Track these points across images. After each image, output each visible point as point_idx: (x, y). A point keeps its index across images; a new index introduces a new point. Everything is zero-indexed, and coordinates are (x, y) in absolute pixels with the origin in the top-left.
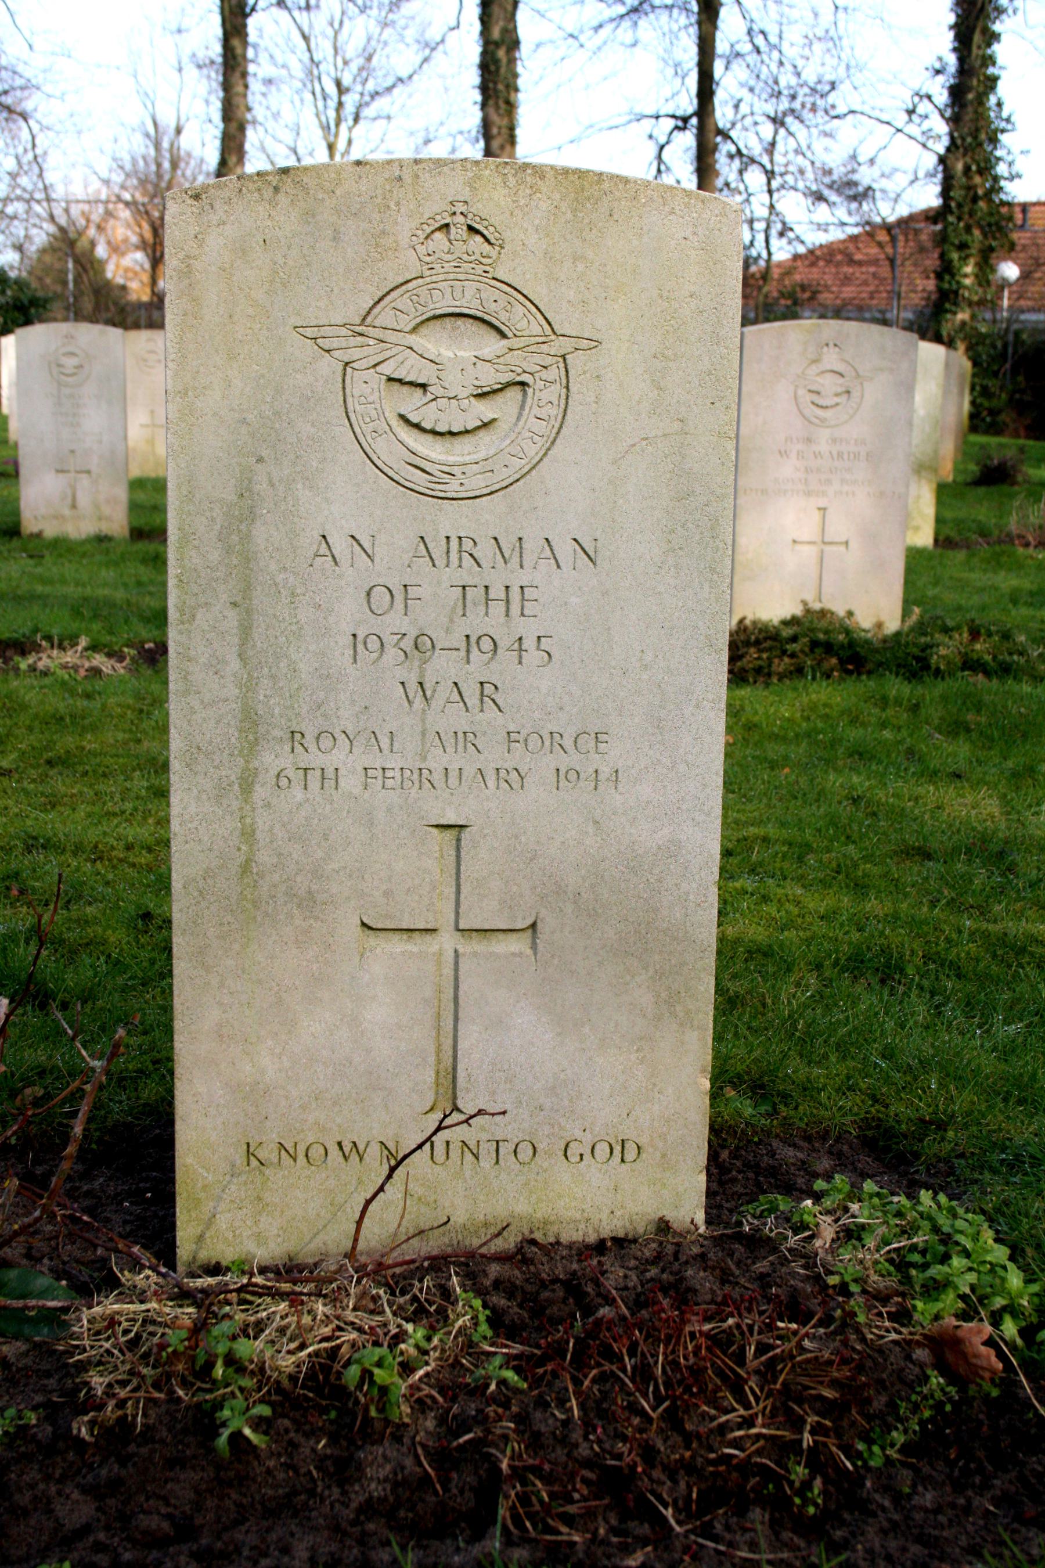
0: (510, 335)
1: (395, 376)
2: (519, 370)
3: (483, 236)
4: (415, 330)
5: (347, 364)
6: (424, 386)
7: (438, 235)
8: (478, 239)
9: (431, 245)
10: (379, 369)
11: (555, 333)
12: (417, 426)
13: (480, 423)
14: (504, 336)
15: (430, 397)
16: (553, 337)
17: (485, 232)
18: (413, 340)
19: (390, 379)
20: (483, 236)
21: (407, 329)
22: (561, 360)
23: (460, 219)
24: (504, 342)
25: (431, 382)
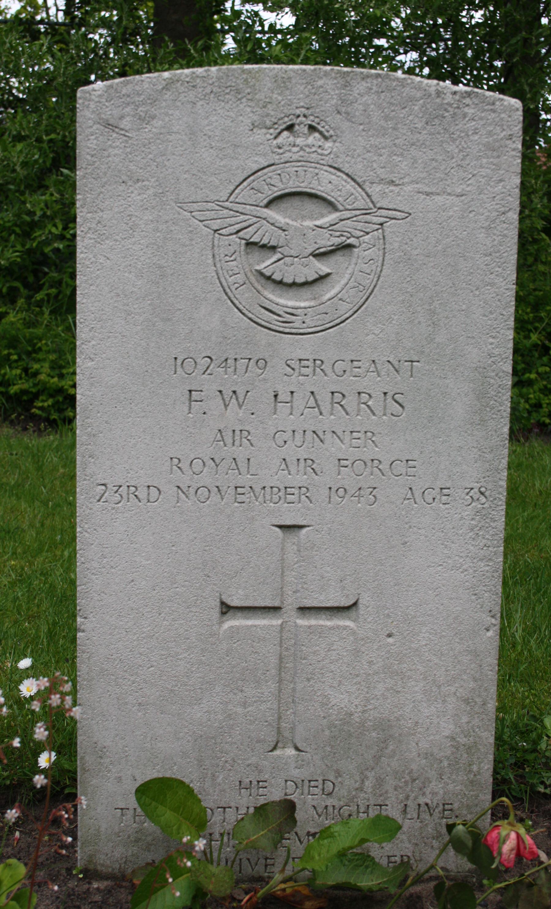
0: (341, 208)
1: (252, 240)
2: (349, 235)
3: (321, 133)
4: (267, 206)
5: (215, 231)
6: (273, 248)
7: (286, 133)
8: (317, 135)
9: (280, 140)
10: (241, 234)
11: (375, 207)
12: (269, 278)
13: (317, 276)
14: (336, 209)
15: (279, 256)
16: (375, 210)
17: (323, 130)
18: (267, 212)
19: (249, 244)
20: (321, 133)
21: (262, 204)
22: (380, 226)
23: (301, 119)
24: (338, 214)
25: (280, 245)
